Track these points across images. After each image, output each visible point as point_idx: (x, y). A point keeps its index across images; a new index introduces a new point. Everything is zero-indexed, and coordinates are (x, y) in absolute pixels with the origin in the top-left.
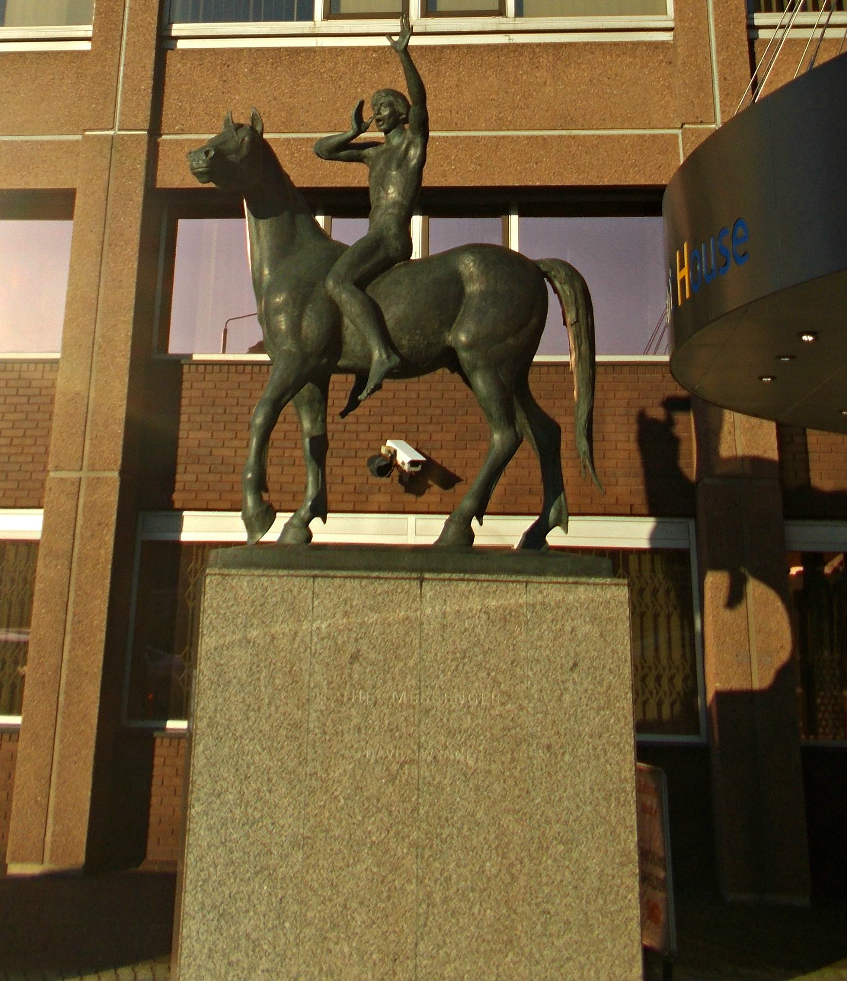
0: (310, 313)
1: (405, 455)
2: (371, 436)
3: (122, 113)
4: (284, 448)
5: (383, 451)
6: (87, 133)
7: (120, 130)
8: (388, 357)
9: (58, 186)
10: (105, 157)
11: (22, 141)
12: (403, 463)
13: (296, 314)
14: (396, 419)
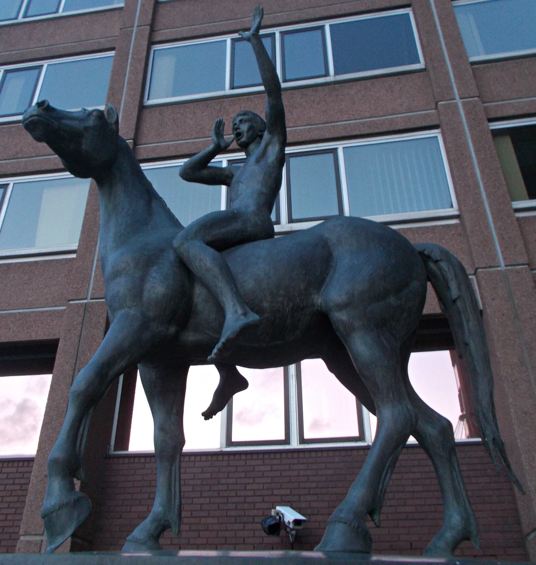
0: (154, 275)
1: (290, 515)
2: (265, 506)
3: (93, 289)
4: (200, 517)
5: (273, 513)
6: (71, 302)
7: (91, 299)
8: (245, 314)
9: (50, 338)
10: (80, 316)
11: (30, 312)
12: (289, 522)
13: (137, 276)
14: (283, 492)
